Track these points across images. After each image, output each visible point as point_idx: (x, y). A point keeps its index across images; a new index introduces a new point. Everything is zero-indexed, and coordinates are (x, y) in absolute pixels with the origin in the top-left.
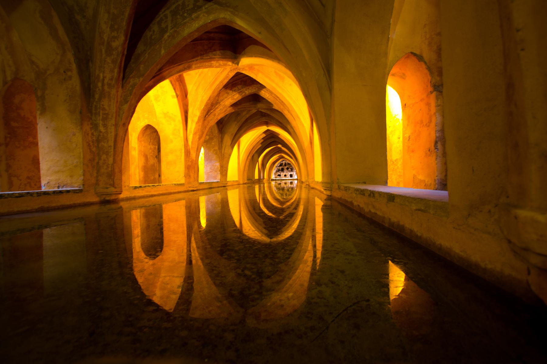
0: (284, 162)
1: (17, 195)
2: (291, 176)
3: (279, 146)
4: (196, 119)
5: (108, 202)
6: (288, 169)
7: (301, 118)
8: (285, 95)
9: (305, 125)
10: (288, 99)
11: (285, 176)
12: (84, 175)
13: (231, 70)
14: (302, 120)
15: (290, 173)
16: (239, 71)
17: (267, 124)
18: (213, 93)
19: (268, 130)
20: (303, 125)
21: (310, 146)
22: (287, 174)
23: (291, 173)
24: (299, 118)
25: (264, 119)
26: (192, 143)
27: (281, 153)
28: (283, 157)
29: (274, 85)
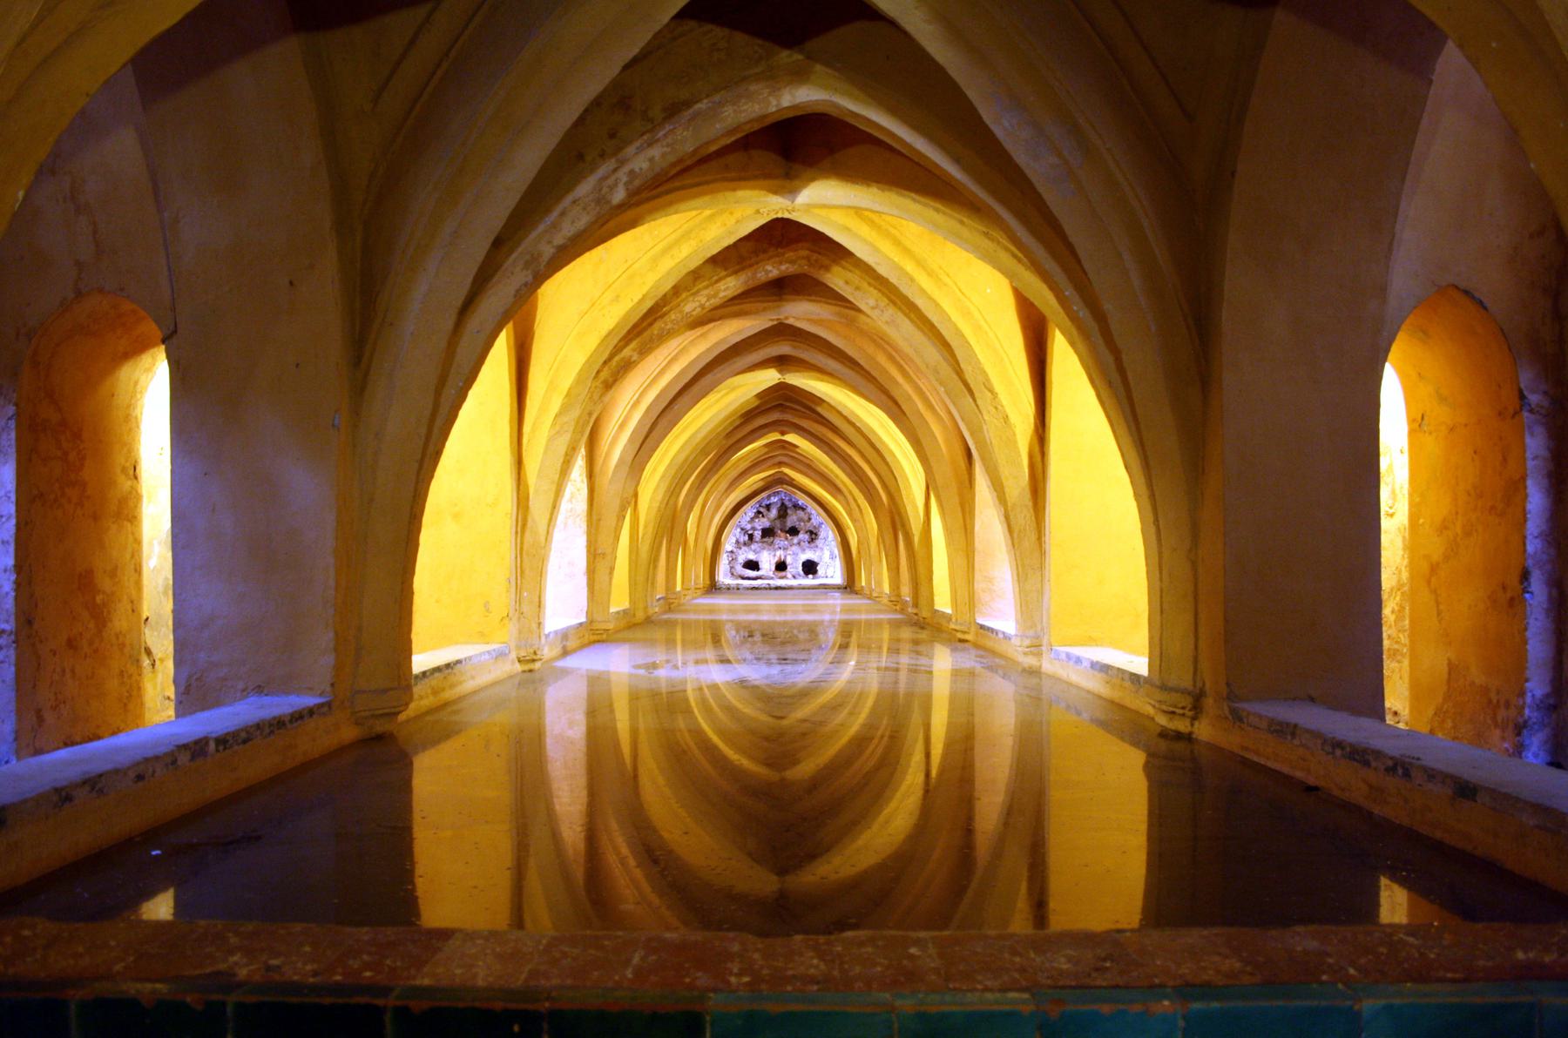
0: (774, 499)
1: (243, 735)
2: (810, 568)
3: (791, 438)
4: (567, 380)
5: (380, 738)
6: (794, 531)
7: (998, 387)
8: (947, 305)
9: (1014, 418)
10: (955, 316)
11: (781, 566)
12: (336, 650)
13: (758, 212)
14: (1004, 398)
15: (804, 557)
16: (786, 215)
17: (781, 362)
18: (656, 286)
19: (781, 387)
20: (1006, 418)
21: (1030, 504)
22: (789, 560)
23: (809, 555)
24: (991, 391)
25: (784, 349)
26: (539, 476)
27: (780, 464)
28: (781, 480)
29: (909, 267)
